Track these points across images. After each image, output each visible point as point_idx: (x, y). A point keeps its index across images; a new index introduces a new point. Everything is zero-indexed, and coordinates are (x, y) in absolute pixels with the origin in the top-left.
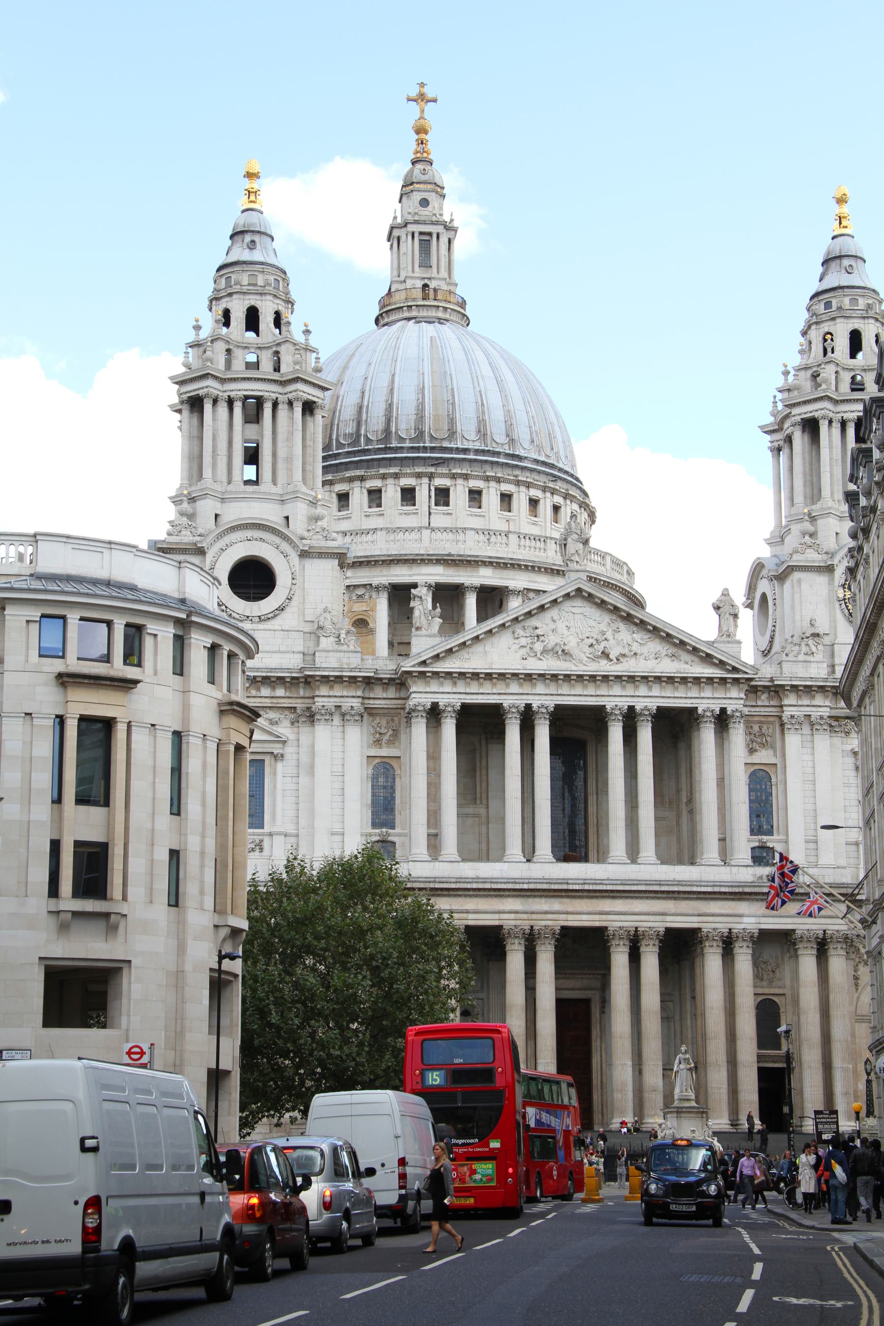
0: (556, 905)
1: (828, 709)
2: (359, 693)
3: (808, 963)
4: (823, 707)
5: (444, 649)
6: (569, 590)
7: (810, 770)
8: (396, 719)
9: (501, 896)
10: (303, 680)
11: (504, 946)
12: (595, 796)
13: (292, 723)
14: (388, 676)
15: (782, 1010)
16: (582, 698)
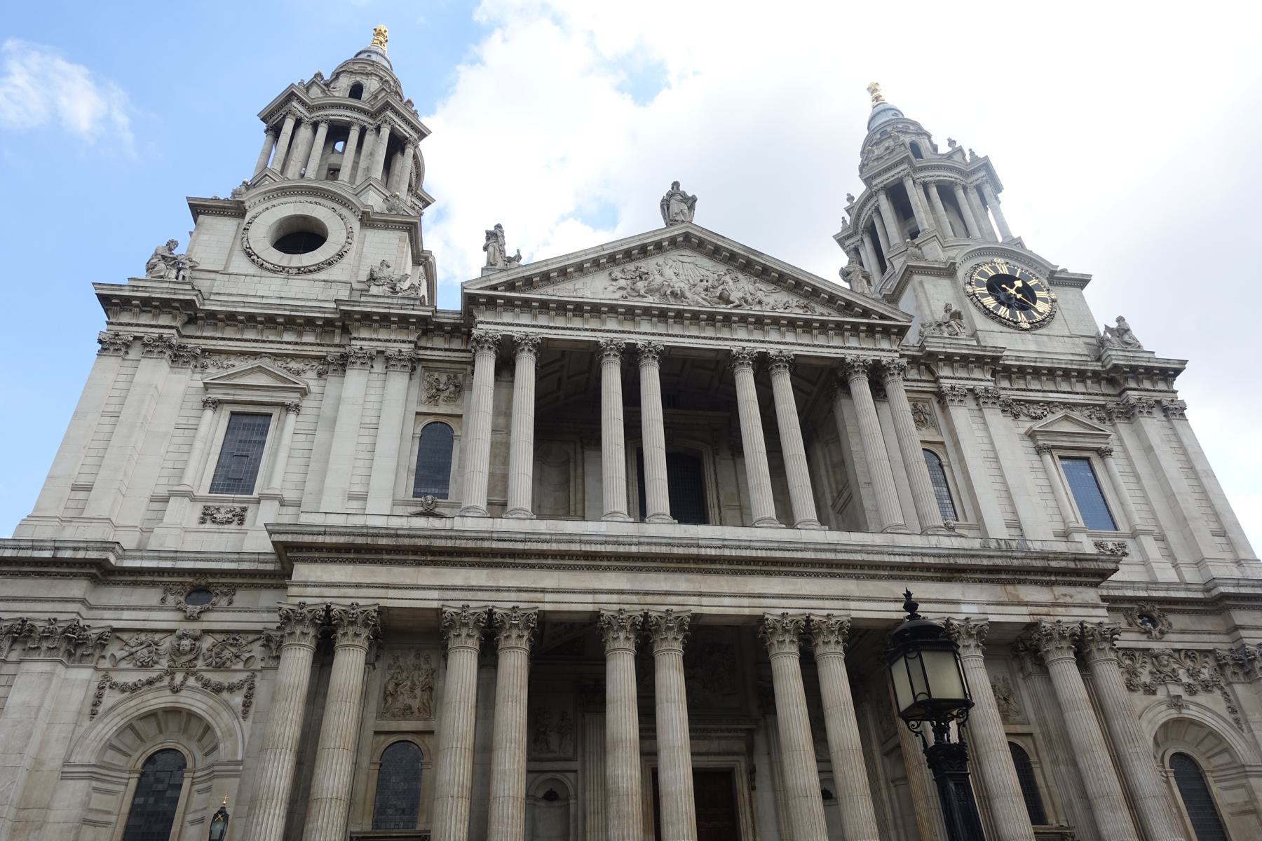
0: (682, 582)
2: (413, 337)
3: (1067, 674)
4: (982, 380)
5: (521, 275)
6: (676, 233)
7: (988, 447)
8: (460, 376)
9: (597, 568)
10: (340, 324)
11: (604, 648)
12: (716, 509)
13: (320, 375)
14: (452, 321)
15: (1033, 759)
16: (700, 341)
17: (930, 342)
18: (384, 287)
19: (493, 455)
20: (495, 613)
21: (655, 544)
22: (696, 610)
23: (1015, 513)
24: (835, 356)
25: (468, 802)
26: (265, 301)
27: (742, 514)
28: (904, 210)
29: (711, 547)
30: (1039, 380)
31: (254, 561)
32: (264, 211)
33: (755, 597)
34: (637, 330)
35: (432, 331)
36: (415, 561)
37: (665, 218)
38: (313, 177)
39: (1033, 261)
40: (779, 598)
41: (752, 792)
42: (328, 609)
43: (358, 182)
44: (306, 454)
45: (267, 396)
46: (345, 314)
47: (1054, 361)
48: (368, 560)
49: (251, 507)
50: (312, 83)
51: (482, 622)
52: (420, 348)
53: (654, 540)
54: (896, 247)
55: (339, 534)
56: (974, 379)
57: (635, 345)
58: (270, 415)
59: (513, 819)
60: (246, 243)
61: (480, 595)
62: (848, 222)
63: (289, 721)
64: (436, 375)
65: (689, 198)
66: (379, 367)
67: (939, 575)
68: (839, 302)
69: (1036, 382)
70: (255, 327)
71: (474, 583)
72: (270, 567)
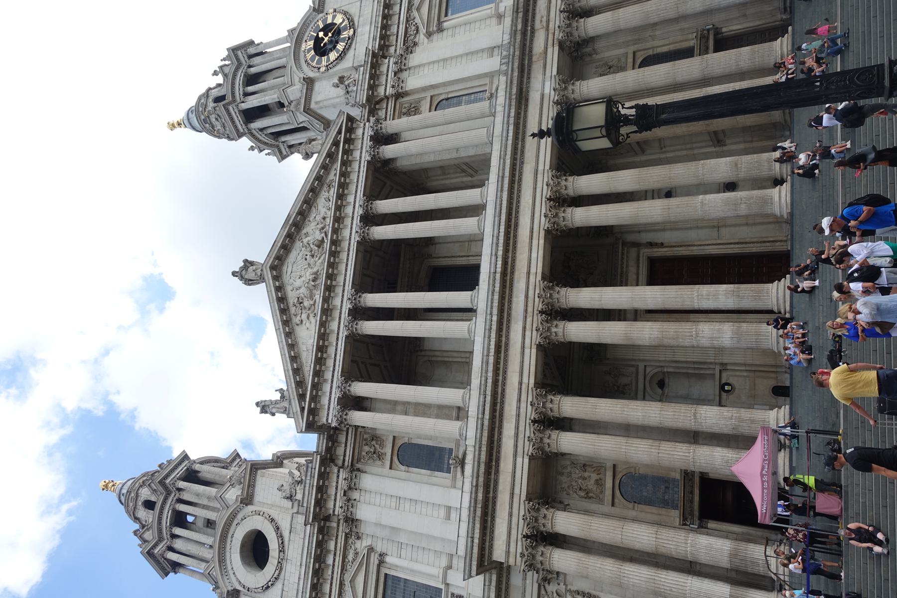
0: (520, 286)
1: (392, 59)
2: (335, 470)
3: (595, 25)
4: (388, 66)
5: (294, 389)
6: (270, 276)
7: (436, 65)
8: (365, 436)
9: (507, 345)
10: (322, 522)
11: (562, 343)
12: (470, 258)
13: (359, 538)
14: (325, 441)
15: (650, 52)
17: (360, 100)
18: (298, 489)
19: (424, 415)
20: (535, 418)
21: (492, 303)
22: (539, 277)
23: (483, 50)
24: (365, 167)
25: (663, 442)
26: (302, 577)
27: (474, 241)
28: (263, 111)
29: (496, 264)
30: (391, 25)
31: (489, 589)
32: (235, 576)
33: (532, 236)
34: (339, 308)
35: (331, 455)
36: (495, 474)
37: (259, 283)
38: (212, 539)
39: (305, 23)
40: (533, 219)
41: (665, 245)
42: (526, 537)
43: (218, 506)
44: (415, 549)
45: (372, 577)
46: (315, 518)
47: (378, 14)
48: (493, 507)
49: (451, 590)
50: (141, 538)
51: (540, 427)
52: (343, 464)
53: (489, 304)
54: (290, 119)
55: (474, 527)
56: (388, 71)
57: (350, 310)
58: (386, 574)
59: (675, 412)
60: (259, 590)
61: (521, 428)
62: (270, 151)
63: (602, 567)
64: (364, 454)
65: (245, 265)
66: (355, 495)
67: (523, 107)
68: (327, 162)
69: (392, 28)
70: (321, 584)
71: (513, 432)
72: (494, 577)
